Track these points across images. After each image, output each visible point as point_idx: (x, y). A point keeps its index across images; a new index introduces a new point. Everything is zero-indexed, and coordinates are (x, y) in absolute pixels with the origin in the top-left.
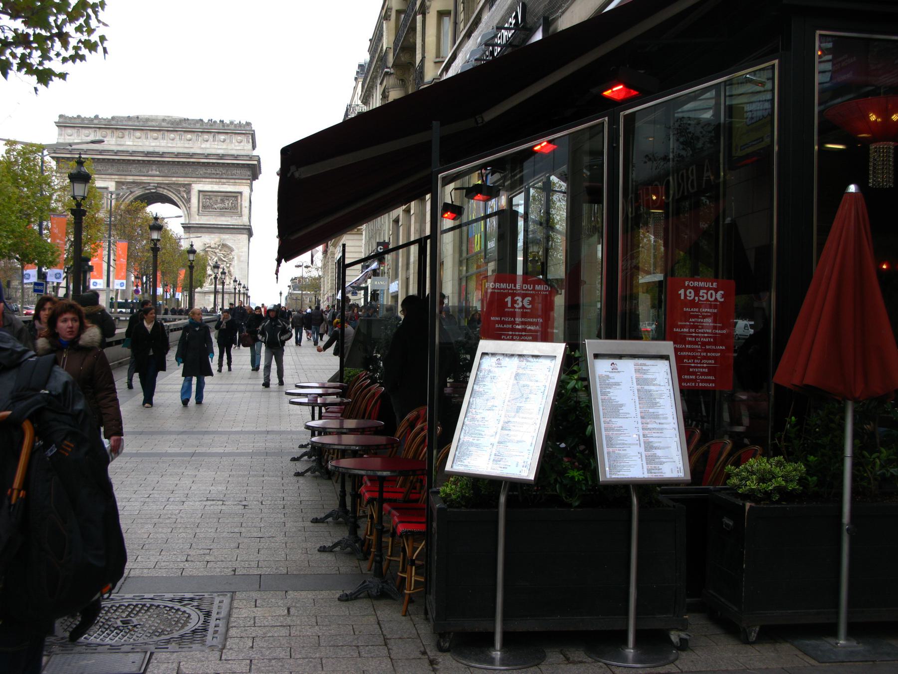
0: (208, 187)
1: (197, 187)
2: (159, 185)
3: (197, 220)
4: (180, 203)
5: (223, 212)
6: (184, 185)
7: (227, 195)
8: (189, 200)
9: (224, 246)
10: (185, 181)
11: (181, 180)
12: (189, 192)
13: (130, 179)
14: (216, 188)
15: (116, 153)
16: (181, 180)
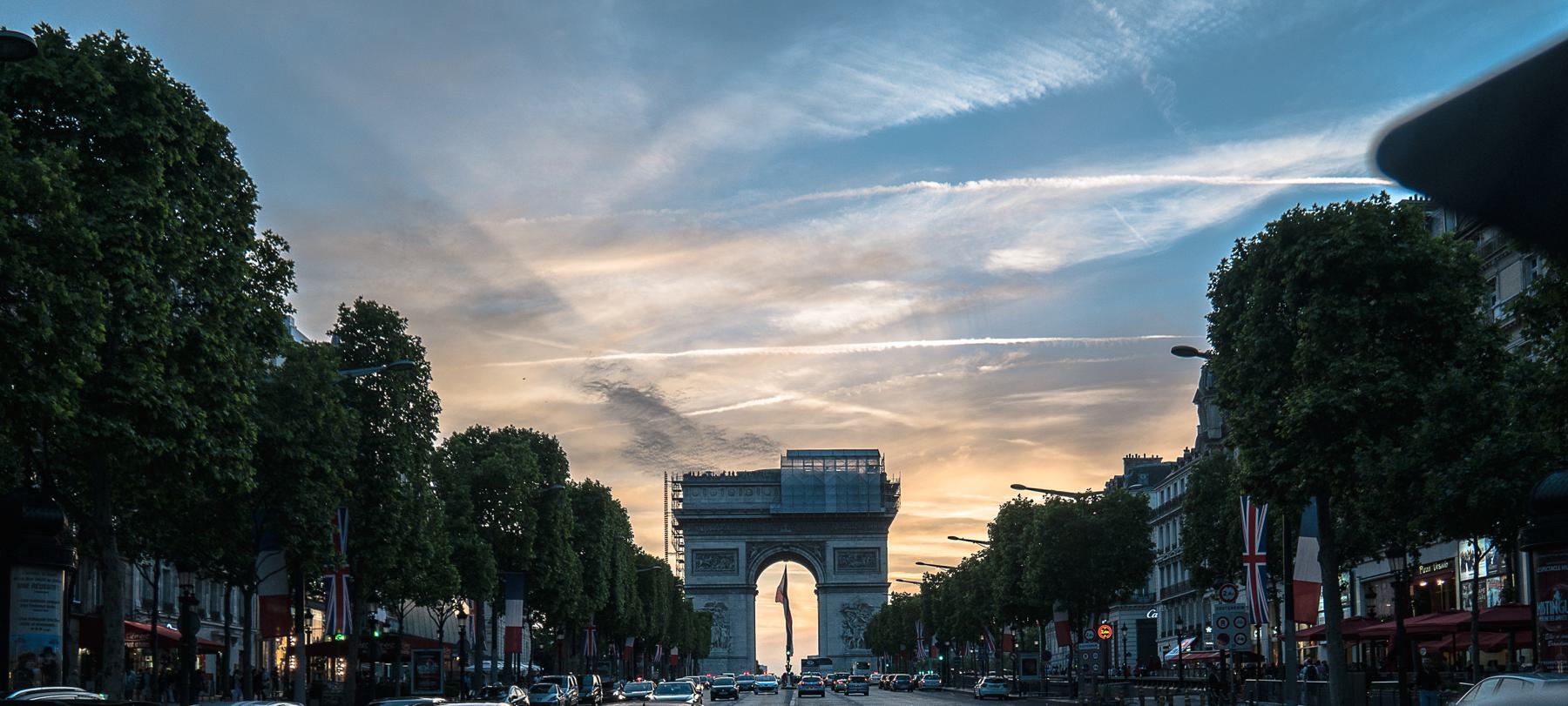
0: (843, 544)
1: (832, 544)
2: (792, 544)
3: (834, 579)
4: (814, 562)
5: (860, 570)
6: (818, 543)
7: (863, 552)
8: (823, 559)
9: (864, 605)
10: (820, 538)
11: (815, 537)
12: (823, 550)
13: (760, 538)
14: (852, 544)
15: (746, 511)
16: (815, 537)
